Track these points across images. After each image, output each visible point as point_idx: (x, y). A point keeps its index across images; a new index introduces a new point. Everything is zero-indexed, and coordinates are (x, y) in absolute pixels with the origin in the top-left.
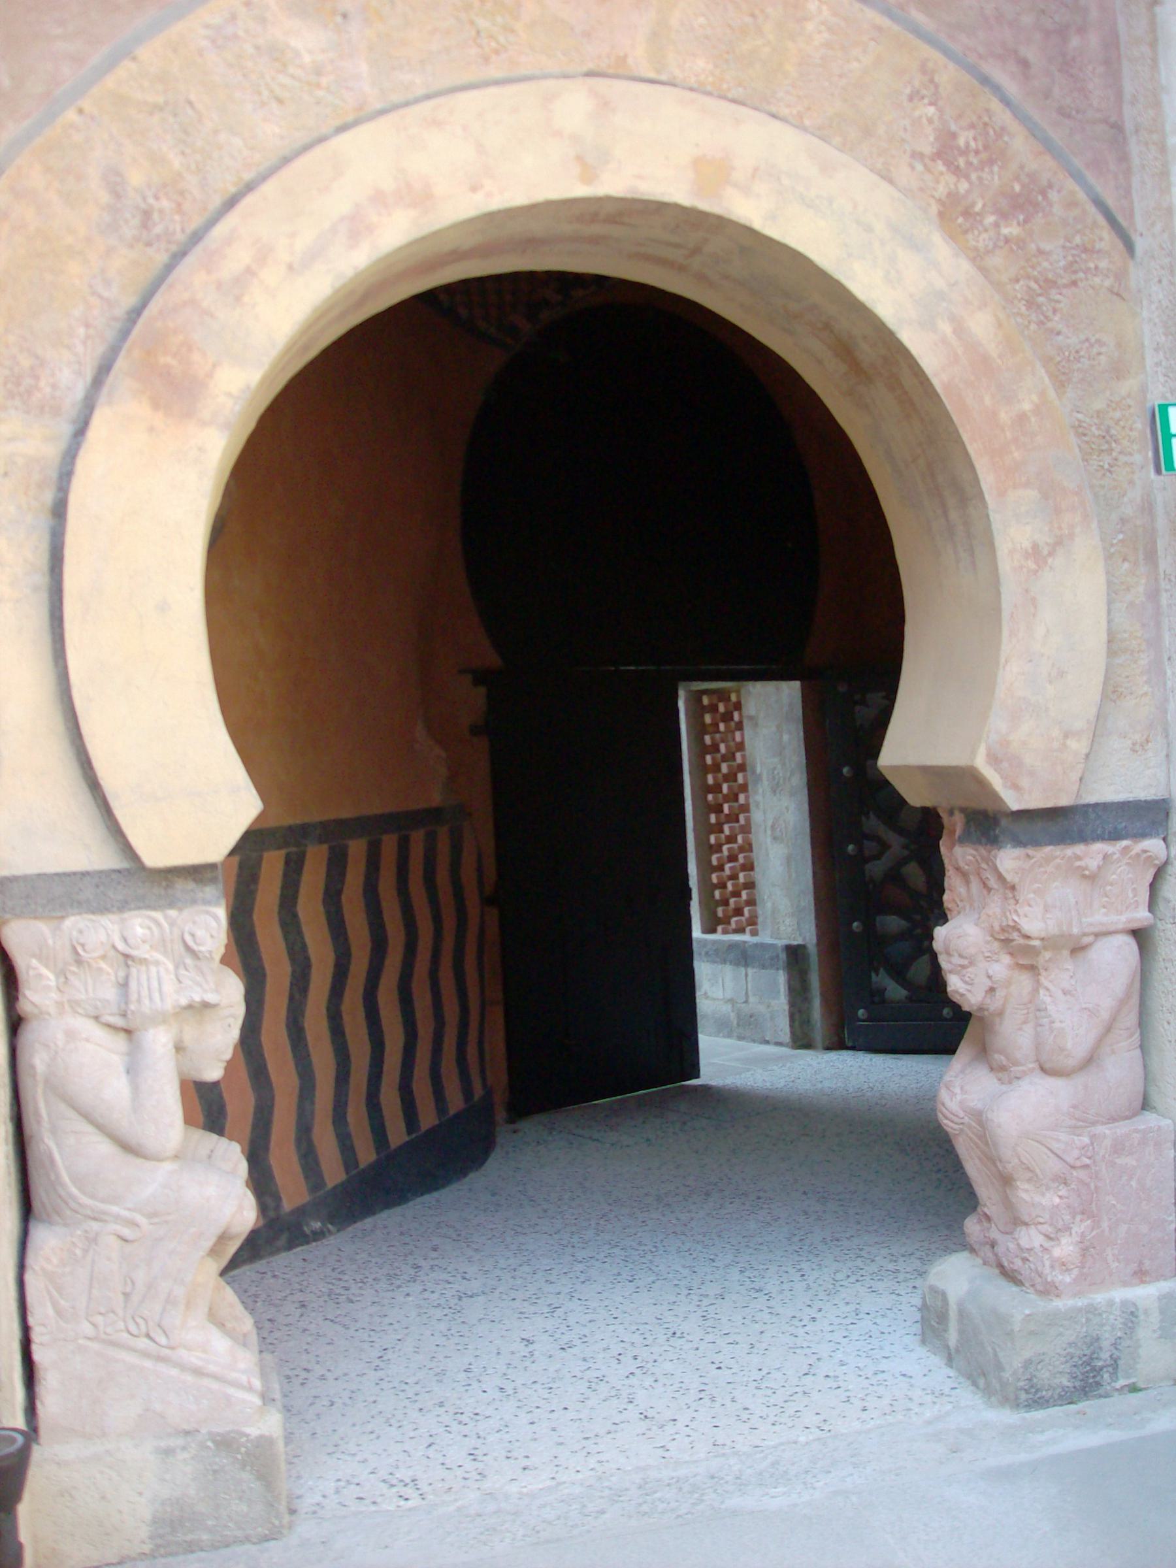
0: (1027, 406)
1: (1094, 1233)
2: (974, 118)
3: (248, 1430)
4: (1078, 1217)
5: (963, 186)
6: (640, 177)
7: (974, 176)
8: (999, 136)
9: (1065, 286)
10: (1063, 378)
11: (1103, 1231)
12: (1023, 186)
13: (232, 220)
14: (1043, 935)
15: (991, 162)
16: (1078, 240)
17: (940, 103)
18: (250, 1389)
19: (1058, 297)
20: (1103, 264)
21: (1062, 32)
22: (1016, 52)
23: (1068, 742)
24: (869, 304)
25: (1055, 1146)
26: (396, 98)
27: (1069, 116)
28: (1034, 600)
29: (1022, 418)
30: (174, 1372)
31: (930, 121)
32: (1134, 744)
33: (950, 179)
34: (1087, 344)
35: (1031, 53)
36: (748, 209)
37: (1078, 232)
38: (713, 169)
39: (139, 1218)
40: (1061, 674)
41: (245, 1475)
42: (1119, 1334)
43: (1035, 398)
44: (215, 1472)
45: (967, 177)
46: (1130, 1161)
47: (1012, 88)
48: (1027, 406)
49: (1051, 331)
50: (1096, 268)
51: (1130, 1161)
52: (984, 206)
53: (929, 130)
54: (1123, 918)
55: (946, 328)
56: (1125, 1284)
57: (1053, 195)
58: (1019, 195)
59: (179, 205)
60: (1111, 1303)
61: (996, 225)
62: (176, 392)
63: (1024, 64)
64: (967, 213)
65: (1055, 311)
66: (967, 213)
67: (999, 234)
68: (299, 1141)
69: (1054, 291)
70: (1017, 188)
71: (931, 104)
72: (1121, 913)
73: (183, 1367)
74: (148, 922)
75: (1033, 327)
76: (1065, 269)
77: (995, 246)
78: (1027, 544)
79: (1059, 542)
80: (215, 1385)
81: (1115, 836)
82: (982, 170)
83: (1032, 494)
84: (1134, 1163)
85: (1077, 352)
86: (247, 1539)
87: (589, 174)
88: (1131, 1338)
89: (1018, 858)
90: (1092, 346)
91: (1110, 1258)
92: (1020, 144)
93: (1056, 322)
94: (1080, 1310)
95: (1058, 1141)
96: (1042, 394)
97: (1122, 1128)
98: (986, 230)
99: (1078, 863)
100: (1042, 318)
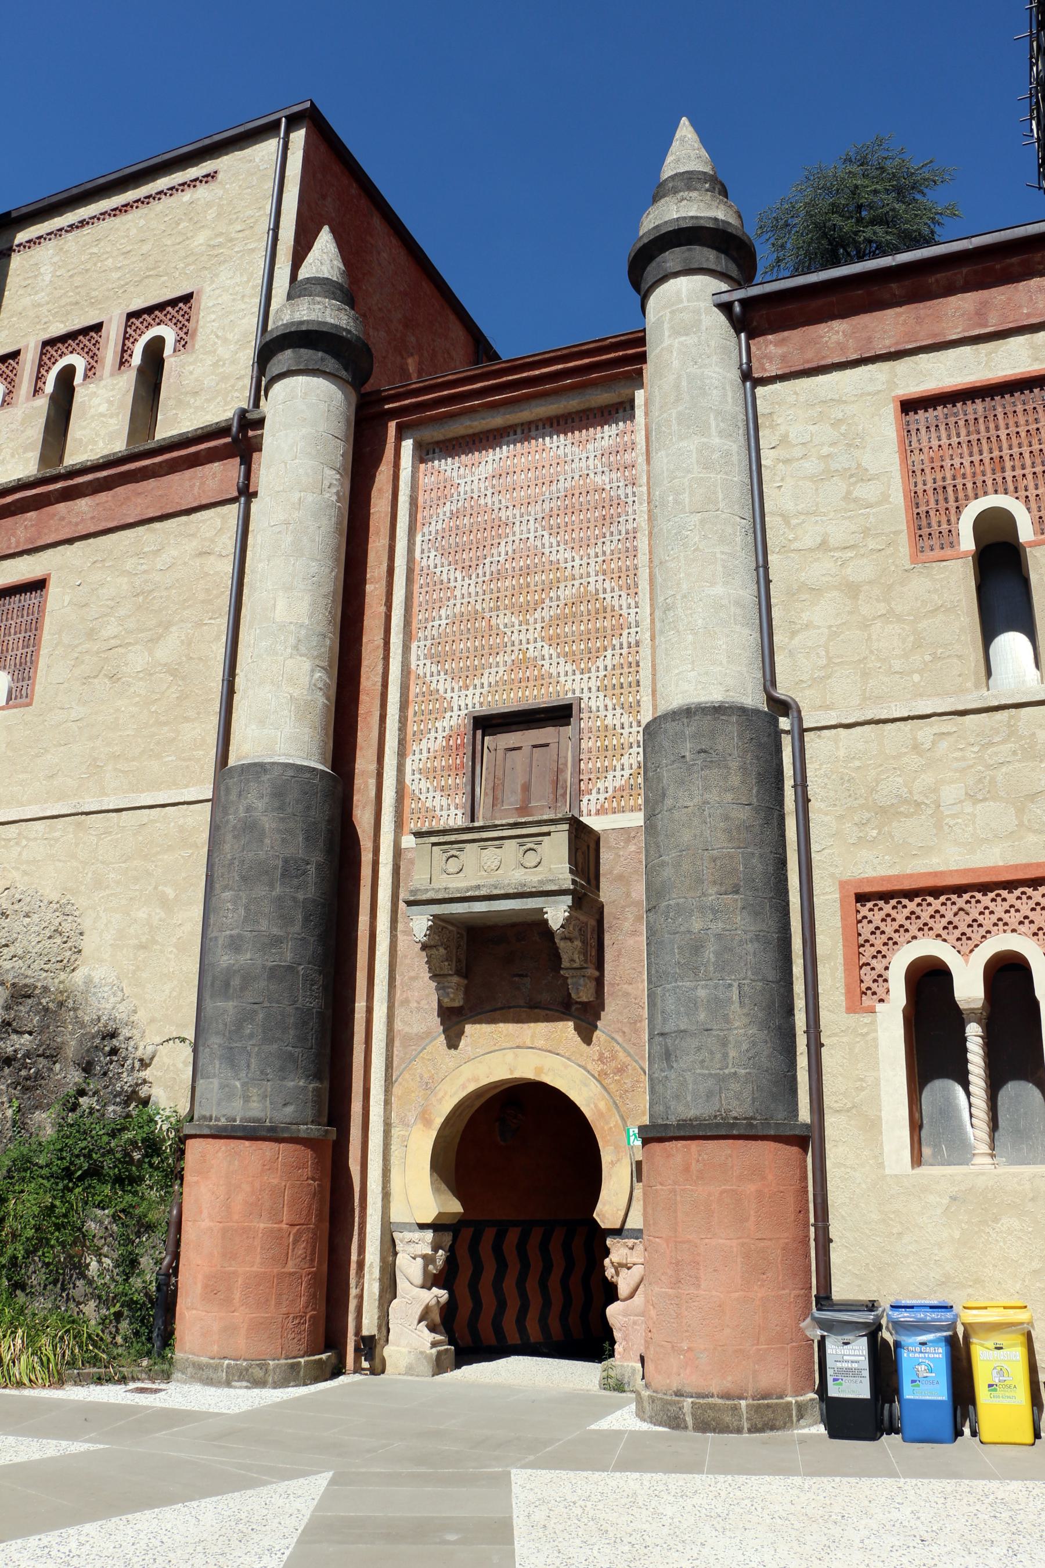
21: (635, 1023)
35: (626, 1029)
38: (539, 1070)
47: (620, 1040)
55: (592, 1106)
62: (427, 1123)
68: (540, 1321)
81: (637, 1238)
87: (511, 1073)
92: (621, 1055)
93: (627, 1101)
97: (636, 1318)
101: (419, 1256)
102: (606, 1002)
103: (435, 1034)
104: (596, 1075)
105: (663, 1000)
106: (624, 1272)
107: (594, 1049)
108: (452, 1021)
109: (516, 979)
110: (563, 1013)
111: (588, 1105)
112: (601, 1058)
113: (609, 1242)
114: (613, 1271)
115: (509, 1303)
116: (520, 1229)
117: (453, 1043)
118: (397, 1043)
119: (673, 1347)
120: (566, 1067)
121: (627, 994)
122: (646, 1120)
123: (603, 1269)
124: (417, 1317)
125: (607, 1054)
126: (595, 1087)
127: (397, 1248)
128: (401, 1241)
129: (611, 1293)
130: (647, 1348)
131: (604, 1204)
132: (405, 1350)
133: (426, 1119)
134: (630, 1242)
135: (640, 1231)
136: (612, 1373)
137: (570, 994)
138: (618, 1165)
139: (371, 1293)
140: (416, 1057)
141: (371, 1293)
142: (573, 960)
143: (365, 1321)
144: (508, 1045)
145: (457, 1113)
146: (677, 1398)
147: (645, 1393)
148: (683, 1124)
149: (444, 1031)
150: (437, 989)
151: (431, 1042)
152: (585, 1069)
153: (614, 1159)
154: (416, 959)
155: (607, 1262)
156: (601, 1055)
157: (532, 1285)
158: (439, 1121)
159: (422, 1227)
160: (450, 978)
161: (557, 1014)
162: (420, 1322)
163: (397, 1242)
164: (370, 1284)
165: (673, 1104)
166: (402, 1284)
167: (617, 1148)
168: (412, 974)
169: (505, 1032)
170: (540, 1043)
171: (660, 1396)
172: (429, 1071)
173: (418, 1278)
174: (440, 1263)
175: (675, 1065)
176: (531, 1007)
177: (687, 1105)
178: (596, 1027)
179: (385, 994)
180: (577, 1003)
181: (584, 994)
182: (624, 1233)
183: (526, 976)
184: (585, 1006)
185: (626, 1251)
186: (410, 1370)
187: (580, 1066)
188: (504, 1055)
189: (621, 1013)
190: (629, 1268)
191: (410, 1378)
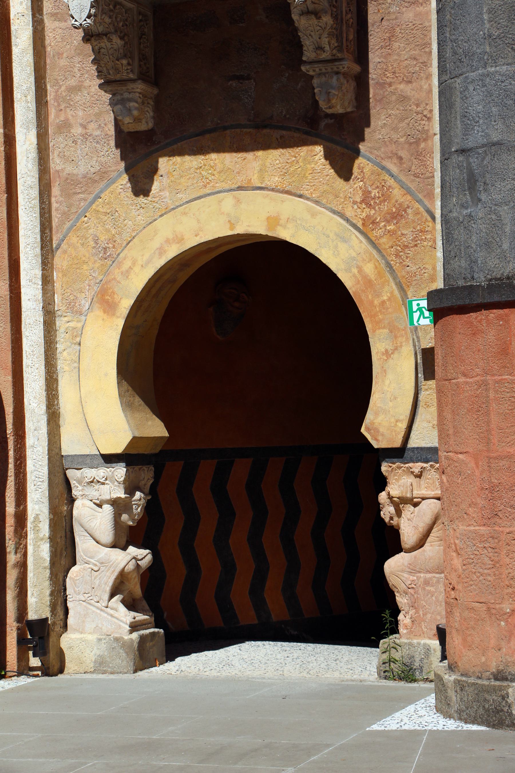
0: (385, 298)
1: (416, 615)
2: (379, 184)
3: (125, 637)
4: (411, 608)
5: (373, 212)
6: (249, 226)
7: (377, 208)
8: (388, 190)
9: (412, 247)
10: (409, 284)
11: (420, 615)
12: (397, 209)
13: (125, 251)
14: (398, 496)
15: (384, 201)
16: (418, 228)
17: (365, 180)
18: (126, 624)
19: (409, 252)
20: (429, 237)
21: (417, 142)
22: (396, 154)
23: (398, 424)
24: (327, 264)
25: (402, 578)
26: (177, 204)
27: (418, 177)
28: (385, 371)
29: (383, 302)
30: (106, 615)
31: (361, 188)
32: (433, 425)
33: (367, 210)
34: (419, 269)
35: (403, 154)
36: (286, 234)
37: (419, 224)
39: (98, 564)
40: (395, 398)
41: (121, 651)
42: (423, 657)
43: (388, 294)
44: (113, 648)
45: (374, 208)
46: (432, 589)
47: (394, 169)
48: (385, 298)
49: (405, 265)
50: (426, 238)
51: (432, 589)
52: (380, 219)
53: (360, 192)
54: (433, 493)
55: (355, 271)
56: (430, 638)
57: (409, 211)
58: (395, 213)
59: (114, 246)
60: (419, 644)
61: (385, 226)
63: (401, 158)
64: (373, 223)
65: (407, 257)
66: (373, 223)
67: (386, 229)
69: (407, 250)
70: (394, 210)
71: (361, 181)
72: (433, 491)
73: (107, 613)
74: (105, 471)
75: (398, 265)
76: (412, 240)
77: (384, 234)
78: (383, 350)
79: (396, 349)
81: (426, 462)
82: (381, 205)
83: (386, 331)
84: (434, 590)
85: (415, 273)
87: (232, 228)
88: (428, 659)
89: (386, 466)
90: (422, 270)
91: (423, 627)
92: (397, 192)
93: (407, 262)
94: (406, 643)
95: (403, 576)
96: (392, 293)
97: (428, 576)
98: (381, 229)
99: (411, 470)
100: (401, 261)
101: (108, 502)
102: (373, 112)
103: (114, 175)
104: (360, 225)
105: (464, 98)
106: (408, 510)
107: (354, 188)
108: (140, 153)
109: (234, 84)
110: (307, 133)
111: (348, 270)
112: (366, 200)
113: (385, 468)
114: (392, 509)
117: (141, 187)
118: (55, 191)
119: (489, 609)
120: (314, 215)
121: (403, 99)
122: (439, 284)
123: (377, 507)
124: (108, 589)
125: (375, 193)
126: (358, 243)
127: (74, 492)
128: (80, 482)
129: (389, 541)
130: (449, 613)
131: (377, 414)
132: (92, 638)
133: (107, 302)
134: (417, 467)
135: (434, 451)
136: (396, 655)
137: (316, 102)
138: (395, 356)
139: (38, 558)
140: (86, 210)
141: (38, 558)
142: (320, 48)
143: (31, 600)
144: (227, 187)
145: (154, 291)
146: (498, 683)
147: (450, 678)
148: (498, 284)
149: (127, 170)
150: (113, 103)
151: (108, 186)
152: (342, 216)
153: (390, 348)
154: (77, 59)
155: (383, 496)
156: (366, 194)
158: (126, 304)
159: (109, 459)
160: (131, 86)
161: (296, 135)
162: (112, 596)
163: (73, 483)
164: (37, 547)
165: (480, 255)
166: (83, 544)
167: (393, 330)
168: (72, 82)
169: (219, 167)
170: (274, 180)
171: (471, 680)
172: (108, 231)
174: (138, 510)
175: (483, 197)
176: (258, 127)
177: (503, 257)
178: (357, 153)
179: (32, 115)
180: (327, 116)
181: (337, 101)
182: (407, 454)
183: (248, 78)
184: (339, 119)
185: (411, 479)
186: (101, 666)
187: (334, 212)
188: (220, 202)
189: (395, 129)
190: (416, 505)
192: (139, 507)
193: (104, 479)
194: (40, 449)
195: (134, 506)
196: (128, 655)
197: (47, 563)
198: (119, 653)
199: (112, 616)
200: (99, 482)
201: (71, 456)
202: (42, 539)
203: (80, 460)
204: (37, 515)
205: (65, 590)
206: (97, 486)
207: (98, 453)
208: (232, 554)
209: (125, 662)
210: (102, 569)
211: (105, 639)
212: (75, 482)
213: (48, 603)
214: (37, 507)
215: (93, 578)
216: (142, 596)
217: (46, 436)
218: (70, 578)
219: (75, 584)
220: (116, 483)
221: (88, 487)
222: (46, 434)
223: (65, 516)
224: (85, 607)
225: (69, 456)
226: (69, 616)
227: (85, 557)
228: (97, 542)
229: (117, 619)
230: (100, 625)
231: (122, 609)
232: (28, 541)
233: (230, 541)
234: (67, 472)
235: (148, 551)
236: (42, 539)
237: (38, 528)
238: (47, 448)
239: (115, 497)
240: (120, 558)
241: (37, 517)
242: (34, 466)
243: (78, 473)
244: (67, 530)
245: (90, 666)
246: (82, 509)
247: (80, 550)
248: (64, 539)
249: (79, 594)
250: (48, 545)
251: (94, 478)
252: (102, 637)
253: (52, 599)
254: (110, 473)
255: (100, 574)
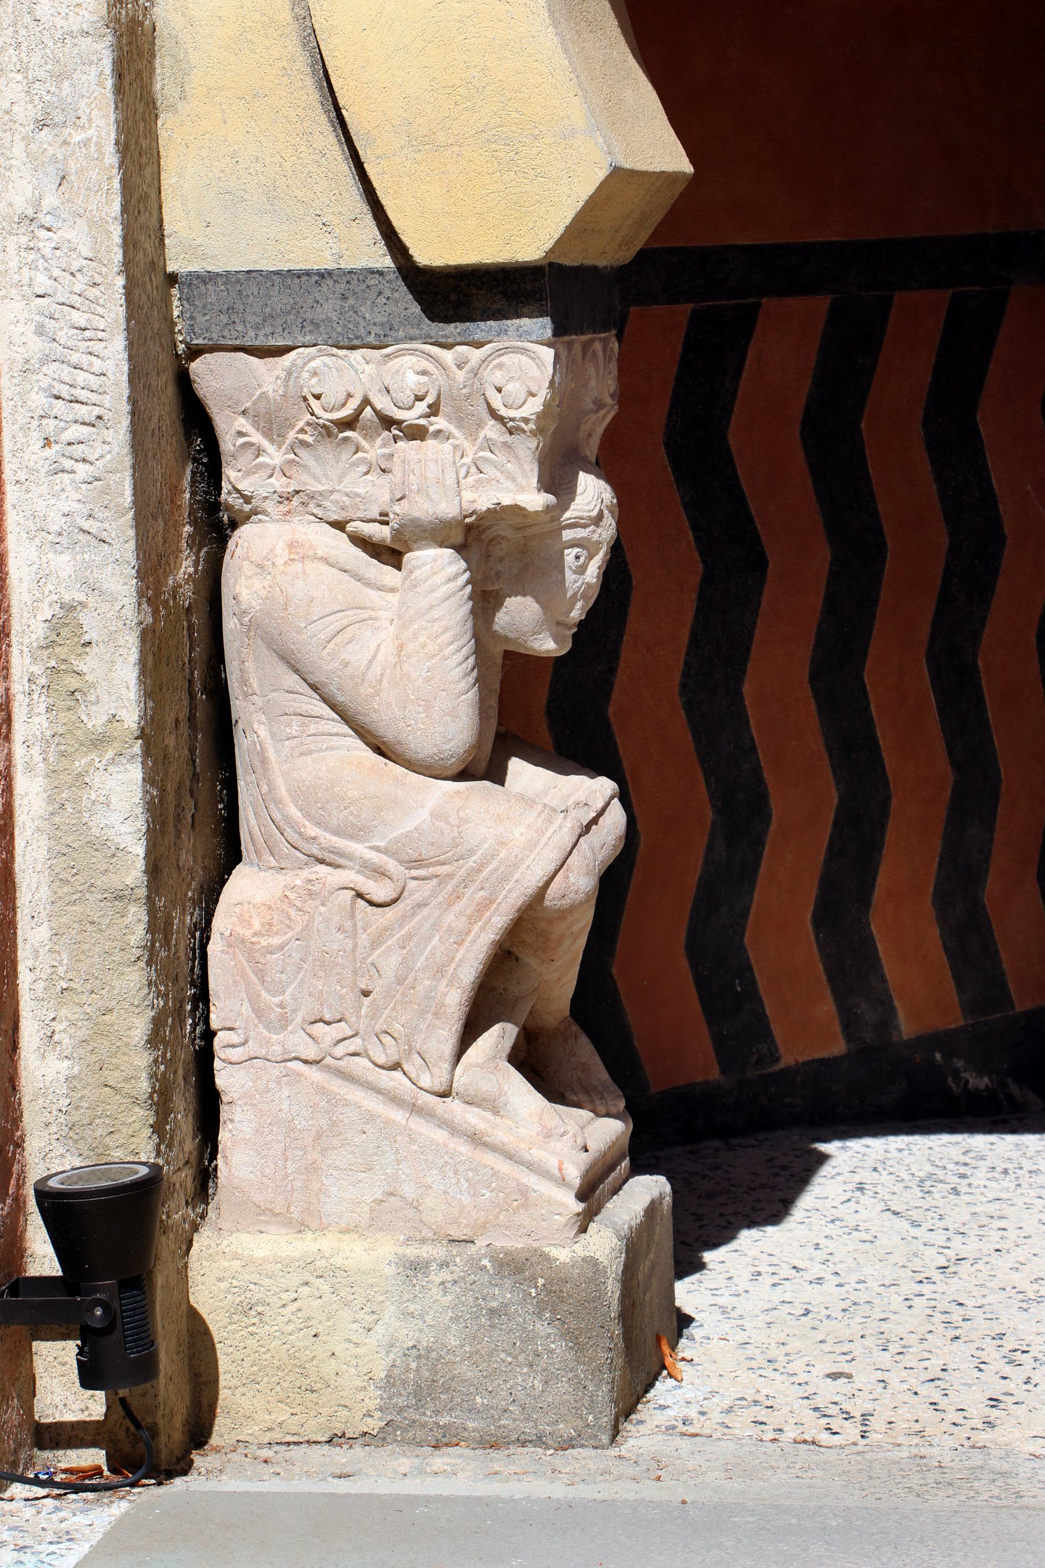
3: (554, 1252)
18: (562, 1182)
30: (440, 1135)
39: (392, 866)
41: (542, 1328)
44: (492, 1312)
68: (943, 899)
73: (453, 1129)
74: (426, 364)
80: (504, 1167)
86: (539, 1441)
101: (438, 533)
115: (780, 804)
116: (821, 304)
124: (455, 1000)
127: (237, 478)
128: (272, 424)
132: (374, 1255)
141: (77, 847)
157: (896, 677)
159: (457, 297)
162: (470, 1031)
163: (231, 428)
173: (445, 710)
174: (583, 574)
186: (421, 1409)
191: (456, 1476)
192: (590, 557)
193: (422, 407)
194: (76, 235)
195: (570, 555)
196: (578, 1347)
197: (134, 872)
198: (530, 1338)
199: (476, 1139)
200: (388, 422)
201: (228, 277)
202: (98, 742)
203: (280, 301)
204: (70, 608)
205: (202, 997)
206: (376, 448)
207: (387, 262)
208: (753, 748)
209: (564, 1386)
210: (418, 891)
211: (444, 1264)
212: (242, 423)
213: (144, 1086)
214: (63, 563)
215: (364, 939)
216: (568, 1013)
217: (111, 158)
218: (233, 941)
219: (261, 974)
220: (491, 430)
221: (326, 450)
222: (110, 148)
223: (189, 610)
224: (321, 1090)
225: (209, 278)
226: (223, 1136)
227: (312, 831)
228: (379, 751)
229: (509, 1156)
230: (408, 1190)
231: (521, 1094)
232: (19, 751)
233: (747, 688)
234: (197, 367)
235: (605, 786)
236: (98, 742)
237: (73, 682)
238: (116, 232)
239: (484, 503)
240: (519, 833)
241: (65, 624)
242: (40, 331)
243: (267, 376)
244: (198, 686)
245: (365, 1409)
246: (281, 568)
247: (283, 792)
248: (184, 729)
249: (284, 1023)
250: (135, 773)
251: (366, 402)
252: (426, 1251)
253: (155, 1061)
254: (461, 376)
255: (404, 919)
